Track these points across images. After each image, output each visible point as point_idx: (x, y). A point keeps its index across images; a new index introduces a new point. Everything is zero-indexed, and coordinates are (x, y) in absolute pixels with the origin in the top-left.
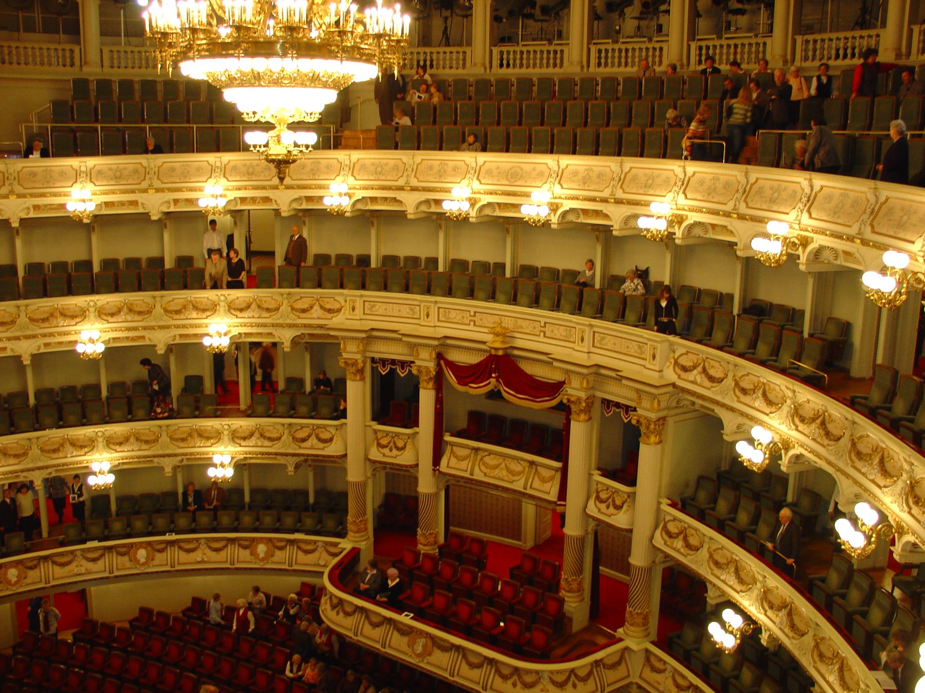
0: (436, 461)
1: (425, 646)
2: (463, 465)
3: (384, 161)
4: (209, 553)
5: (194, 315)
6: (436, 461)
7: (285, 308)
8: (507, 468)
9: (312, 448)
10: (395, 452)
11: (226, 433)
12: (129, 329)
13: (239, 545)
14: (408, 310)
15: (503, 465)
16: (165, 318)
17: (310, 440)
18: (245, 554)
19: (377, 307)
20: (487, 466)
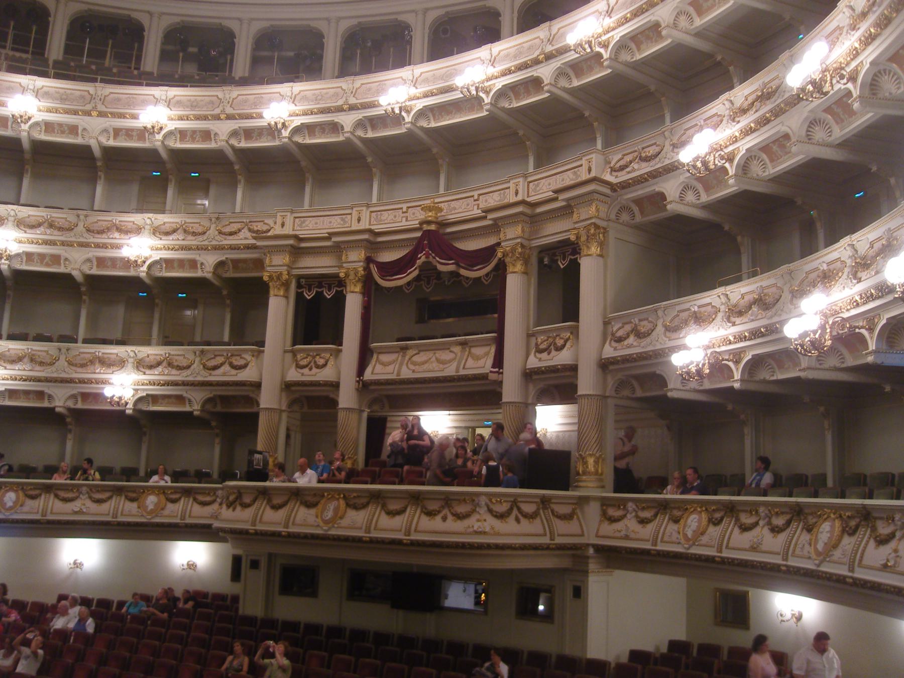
0: (361, 370)
1: (336, 510)
2: (390, 369)
3: (325, 91)
4: (89, 503)
5: (117, 235)
6: (361, 370)
7: (212, 232)
8: (438, 360)
9: (224, 374)
10: (315, 370)
11: (131, 360)
12: (46, 242)
13: (126, 497)
14: (339, 220)
15: (434, 359)
16: (86, 235)
17: (223, 368)
18: (131, 507)
19: (307, 223)
20: (415, 364)
